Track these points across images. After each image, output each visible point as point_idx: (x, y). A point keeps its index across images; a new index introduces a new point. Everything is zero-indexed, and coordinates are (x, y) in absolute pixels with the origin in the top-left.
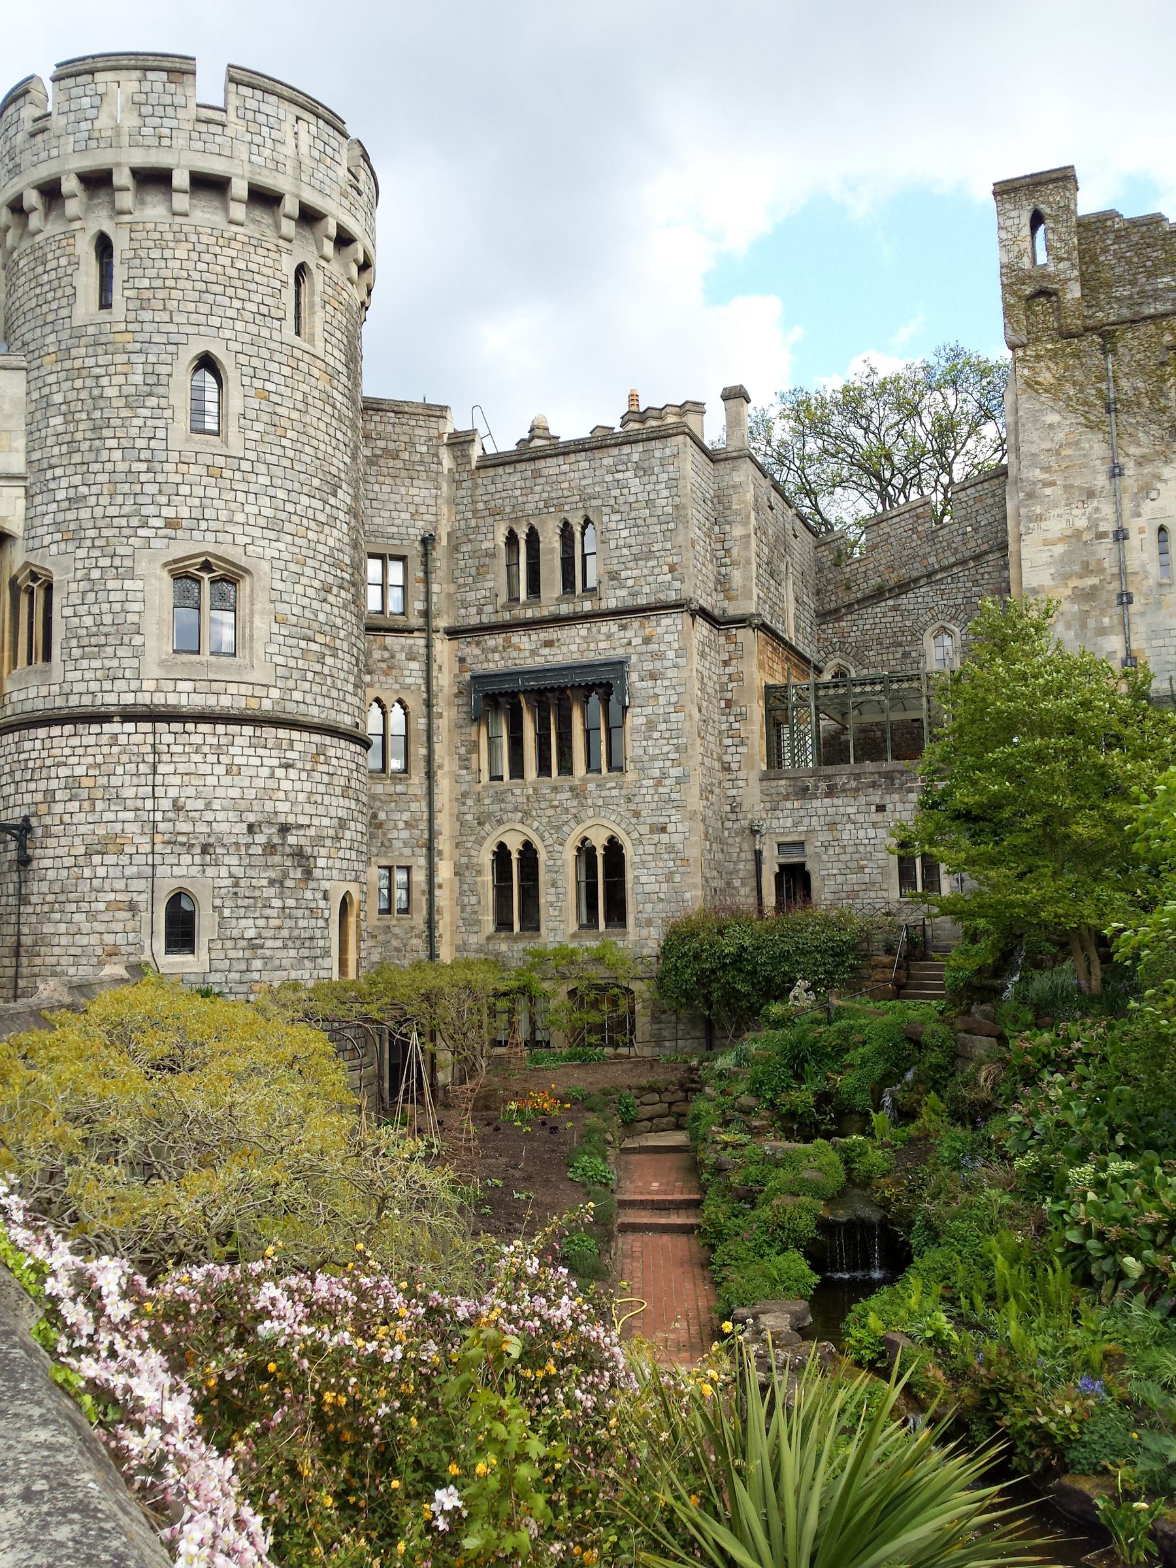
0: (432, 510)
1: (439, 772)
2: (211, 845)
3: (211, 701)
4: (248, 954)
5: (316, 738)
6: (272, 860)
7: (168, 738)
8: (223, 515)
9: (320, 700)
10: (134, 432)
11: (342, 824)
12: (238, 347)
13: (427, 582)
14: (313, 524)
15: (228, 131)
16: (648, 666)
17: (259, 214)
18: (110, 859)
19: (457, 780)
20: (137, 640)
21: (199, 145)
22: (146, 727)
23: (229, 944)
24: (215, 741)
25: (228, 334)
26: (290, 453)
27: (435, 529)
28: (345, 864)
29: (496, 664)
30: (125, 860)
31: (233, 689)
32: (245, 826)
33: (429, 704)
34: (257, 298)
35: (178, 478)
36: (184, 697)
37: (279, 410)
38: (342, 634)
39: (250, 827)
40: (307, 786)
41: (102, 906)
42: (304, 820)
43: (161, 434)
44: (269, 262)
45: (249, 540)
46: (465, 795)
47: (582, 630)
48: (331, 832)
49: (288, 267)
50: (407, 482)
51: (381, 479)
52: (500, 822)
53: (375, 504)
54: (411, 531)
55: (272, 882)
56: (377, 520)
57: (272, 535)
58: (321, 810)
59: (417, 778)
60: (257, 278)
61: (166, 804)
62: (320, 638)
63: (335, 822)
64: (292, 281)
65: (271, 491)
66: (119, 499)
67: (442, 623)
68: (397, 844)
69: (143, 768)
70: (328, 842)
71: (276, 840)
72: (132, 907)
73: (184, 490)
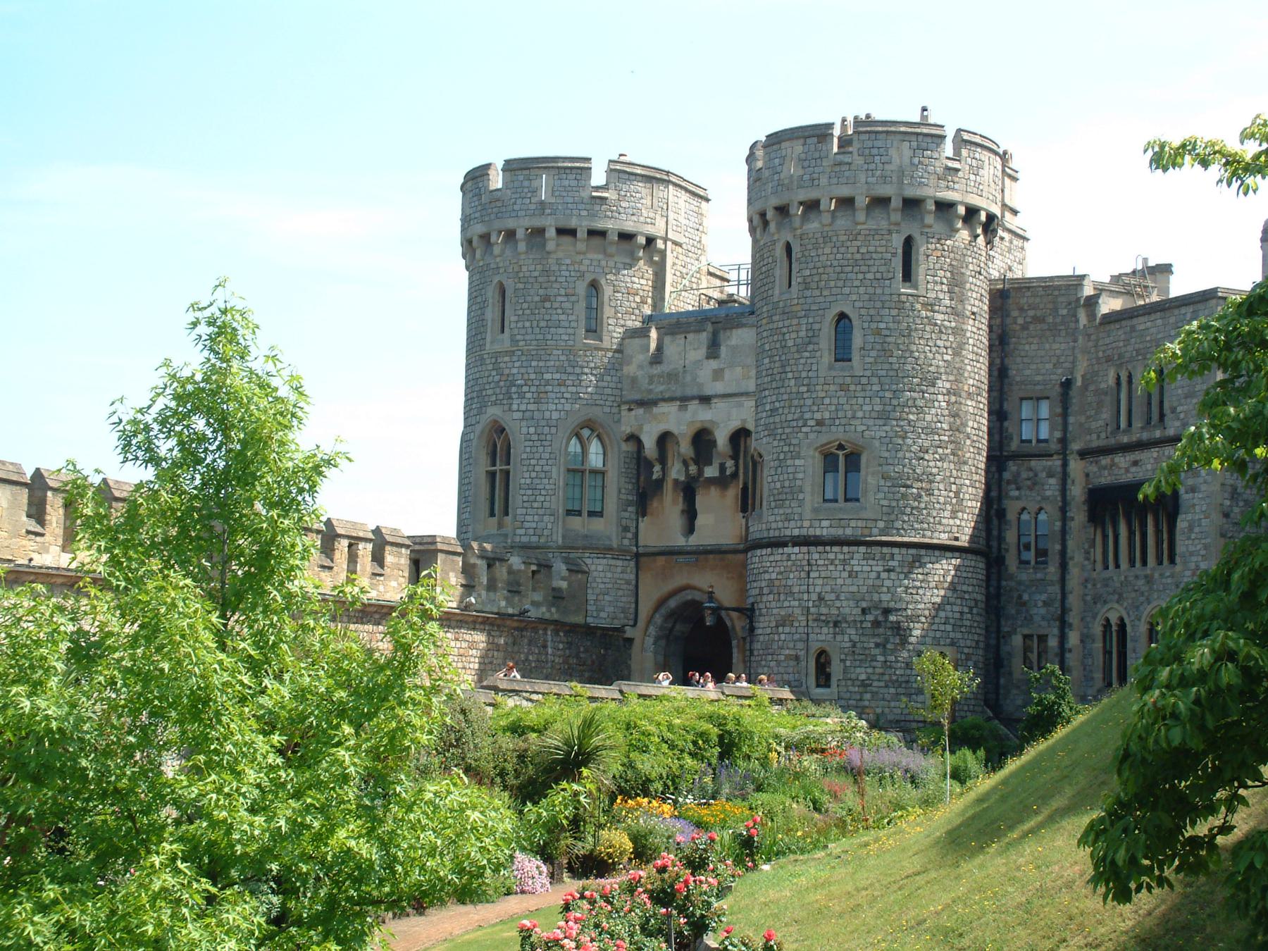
0: (1071, 359)
1: (1071, 563)
2: (839, 622)
3: (840, 532)
4: (861, 689)
6: (877, 631)
7: (816, 556)
8: (849, 414)
10: (801, 367)
12: (861, 304)
13: (1065, 415)
15: (853, 167)
17: (878, 212)
18: (787, 629)
19: (1083, 568)
20: (801, 496)
21: (835, 181)
22: (804, 549)
23: (849, 683)
24: (841, 557)
25: (854, 297)
27: (1072, 373)
28: (938, 634)
29: (1105, 479)
30: (793, 630)
31: (853, 523)
32: (860, 610)
33: (1063, 510)
34: (874, 269)
35: (823, 394)
36: (824, 529)
37: (889, 339)
39: (864, 611)
41: (782, 658)
43: (814, 368)
44: (884, 242)
45: (864, 428)
46: (1086, 581)
47: (1154, 452)
49: (897, 242)
50: (1051, 339)
51: (1030, 340)
52: (1105, 602)
53: (1026, 360)
55: (877, 645)
56: (1027, 372)
57: (881, 422)
59: (1053, 569)
60: (874, 256)
61: (814, 597)
64: (900, 251)
65: (881, 394)
66: (793, 409)
67: (1075, 446)
68: (1037, 619)
69: (803, 575)
71: (881, 618)
72: (797, 658)
73: (827, 401)
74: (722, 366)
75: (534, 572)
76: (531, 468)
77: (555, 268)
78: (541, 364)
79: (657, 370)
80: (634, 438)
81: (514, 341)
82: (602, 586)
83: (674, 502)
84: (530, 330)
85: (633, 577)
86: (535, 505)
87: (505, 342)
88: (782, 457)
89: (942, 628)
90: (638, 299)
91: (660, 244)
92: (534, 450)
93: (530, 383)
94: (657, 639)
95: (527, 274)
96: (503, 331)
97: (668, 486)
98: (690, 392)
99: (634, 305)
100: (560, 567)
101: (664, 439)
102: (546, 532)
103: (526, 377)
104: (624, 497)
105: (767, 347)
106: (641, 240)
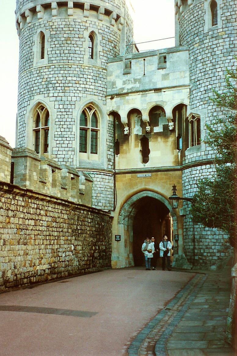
74: (168, 72)
75: (72, 178)
76: (61, 126)
77: (73, 23)
78: (66, 72)
79: (128, 77)
80: (115, 115)
81: (50, 61)
82: (99, 189)
83: (136, 146)
84: (59, 55)
85: (113, 185)
86: (63, 145)
87: (45, 61)
90: (113, 45)
92: (63, 117)
93: (59, 82)
94: (125, 217)
95: (57, 26)
96: (43, 57)
97: (132, 139)
98: (147, 88)
99: (111, 48)
100: (82, 178)
101: (135, 112)
102: (70, 160)
103: (57, 79)
104: (108, 143)
105: (200, 58)
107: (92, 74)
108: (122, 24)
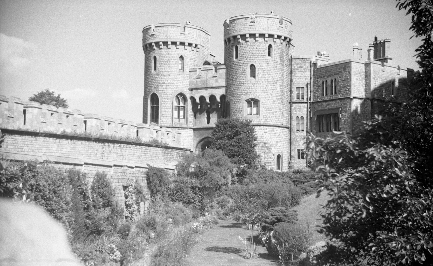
5: (272, 128)
9: (272, 121)
11: (277, 142)
14: (271, 90)
16: (345, 109)
26: (267, 79)
28: (278, 149)
29: (320, 108)
34: (261, 53)
37: (264, 71)
38: (278, 108)
40: (270, 136)
42: (269, 142)
47: (334, 102)
48: (275, 144)
54: (305, 82)
58: (272, 140)
62: (273, 110)
63: (276, 142)
65: (263, 86)
70: (274, 146)
80: (193, 99)
84: (164, 69)
88: (236, 103)
89: (279, 148)
90: (193, 61)
91: (198, 46)
106: (194, 45)
107: (181, 78)
108: (198, 48)
